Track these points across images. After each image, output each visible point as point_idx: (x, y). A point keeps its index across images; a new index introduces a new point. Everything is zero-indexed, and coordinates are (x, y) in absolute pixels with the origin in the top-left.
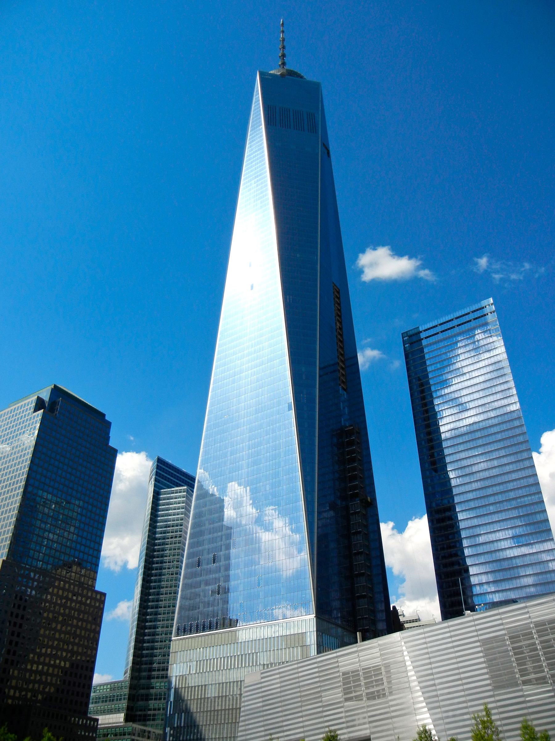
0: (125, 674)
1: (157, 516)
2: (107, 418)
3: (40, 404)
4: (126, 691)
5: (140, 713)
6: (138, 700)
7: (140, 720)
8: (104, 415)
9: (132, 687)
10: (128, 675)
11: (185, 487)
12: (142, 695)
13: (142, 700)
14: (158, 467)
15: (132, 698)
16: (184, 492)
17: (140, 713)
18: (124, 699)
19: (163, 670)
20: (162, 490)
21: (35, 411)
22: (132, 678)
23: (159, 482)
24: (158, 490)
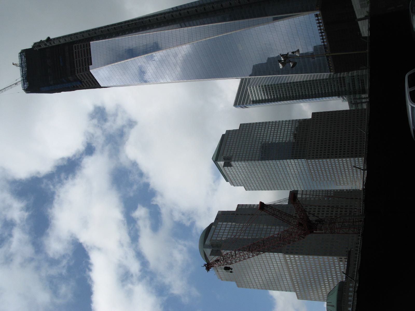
1: (262, 100)
2: (224, 133)
3: (228, 164)
4: (352, 97)
5: (361, 88)
8: (223, 135)
9: (350, 94)
11: (248, 87)
14: (239, 104)
15: (355, 93)
16: (250, 87)
17: (361, 88)
19: (341, 80)
20: (251, 100)
21: (230, 165)
22: (346, 94)
24: (251, 102)
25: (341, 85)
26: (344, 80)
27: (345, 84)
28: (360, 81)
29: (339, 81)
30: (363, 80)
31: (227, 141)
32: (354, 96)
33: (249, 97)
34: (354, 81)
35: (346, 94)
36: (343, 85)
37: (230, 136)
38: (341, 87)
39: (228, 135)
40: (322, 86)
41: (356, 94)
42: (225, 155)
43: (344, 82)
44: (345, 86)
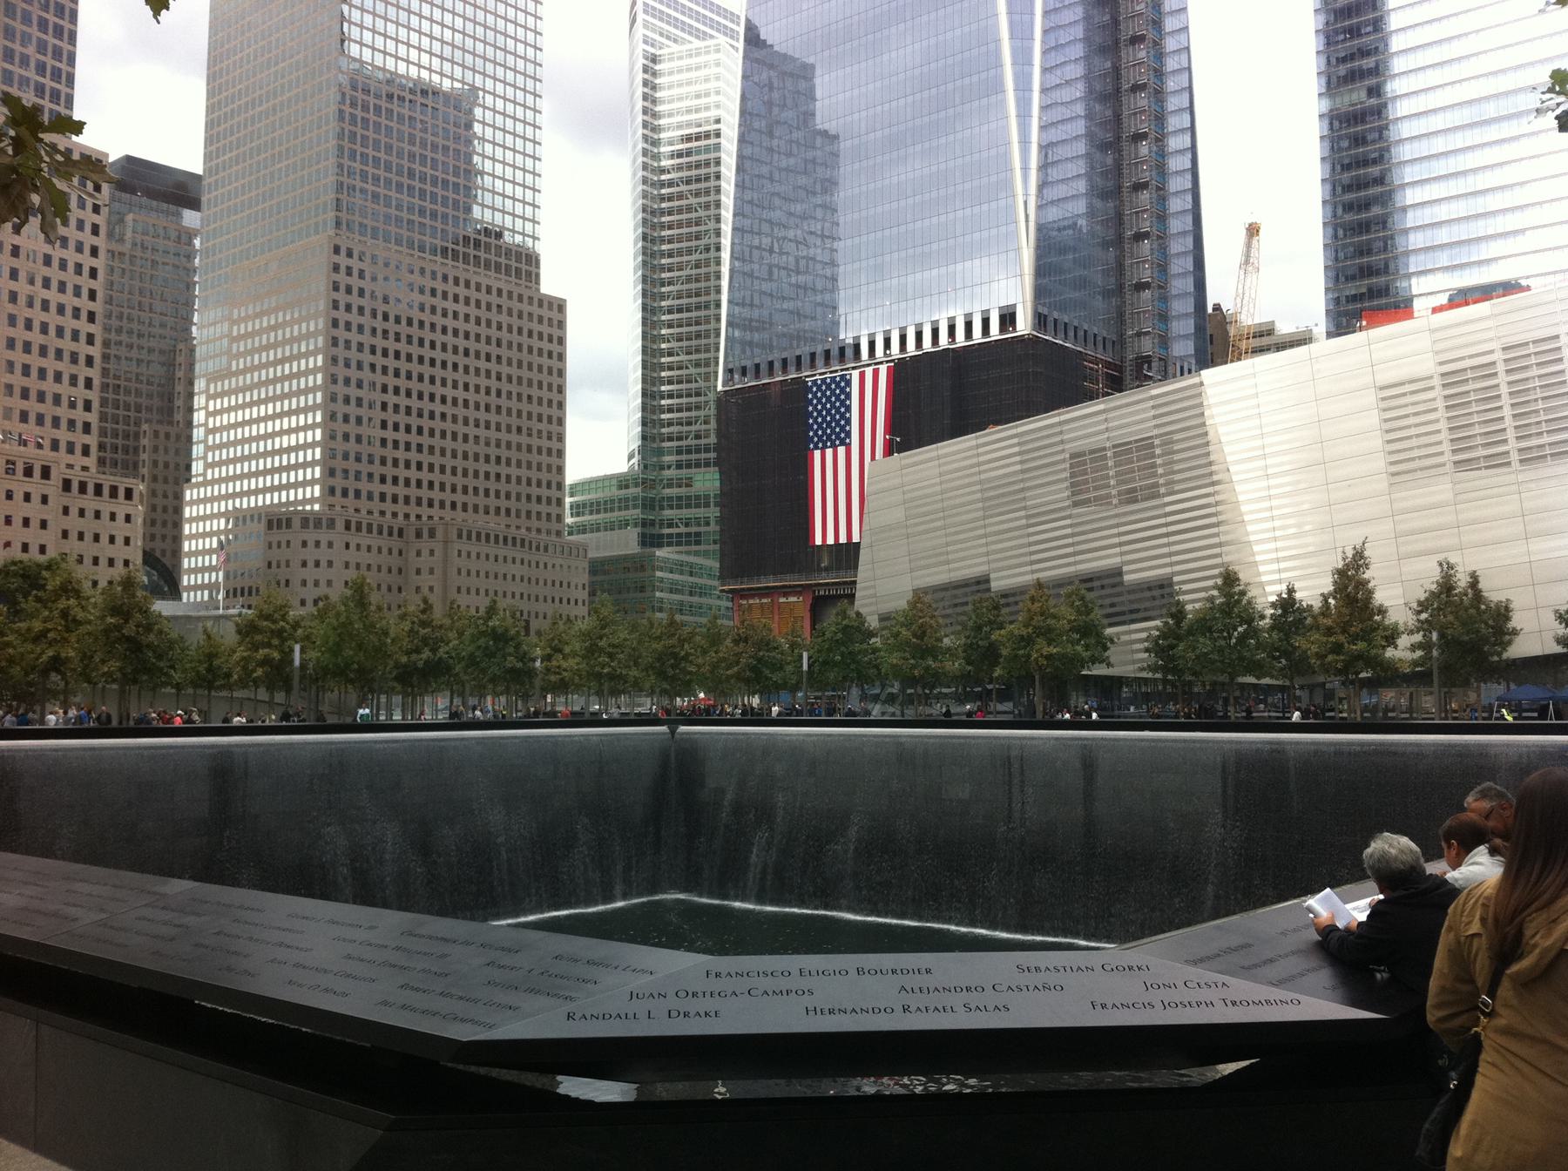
0: (631, 457)
5: (666, 531)
6: (662, 508)
7: (670, 544)
10: (635, 460)
12: (670, 499)
13: (671, 507)
17: (666, 531)
18: (635, 507)
23: (654, 31)
25: (689, 452)
27: (689, 466)
28: (693, 529)
29: (703, 441)
30: (698, 543)
32: (635, 498)
33: (668, 38)
35: (646, 467)
36: (684, 457)
38: (679, 452)
40: (692, 370)
41: (644, 506)
43: (698, 465)
44: (679, 466)
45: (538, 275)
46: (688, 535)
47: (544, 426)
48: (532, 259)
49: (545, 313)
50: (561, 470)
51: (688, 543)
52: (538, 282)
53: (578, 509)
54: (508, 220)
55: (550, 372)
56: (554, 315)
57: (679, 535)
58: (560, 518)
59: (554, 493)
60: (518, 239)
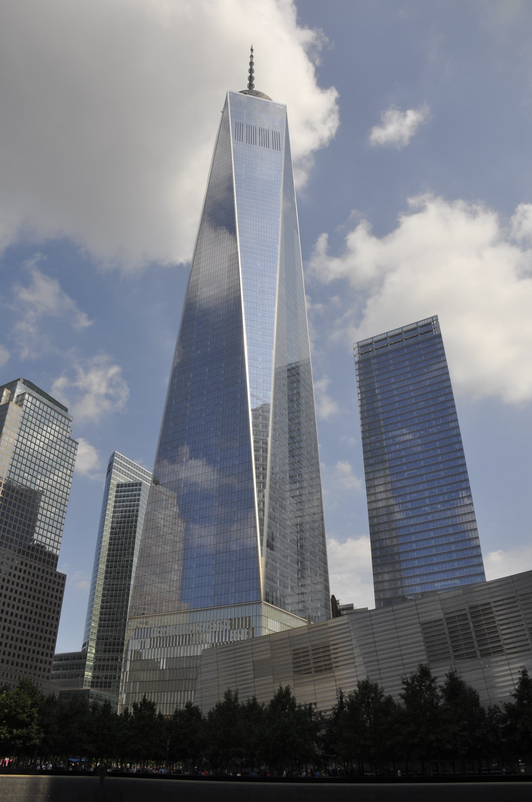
26: (117, 651)
27: (109, 651)
28: (108, 680)
31: (52, 409)
34: (111, 669)
37: (60, 417)
39: (62, 416)
42: (27, 396)
45: (56, 564)
46: (105, 683)
47: (48, 628)
48: (55, 558)
49: (57, 580)
50: (53, 649)
51: (105, 686)
52: (56, 567)
53: (57, 667)
54: (48, 540)
55: (55, 605)
56: (61, 581)
57: (101, 683)
58: (49, 671)
59: (49, 659)
60: (51, 549)
